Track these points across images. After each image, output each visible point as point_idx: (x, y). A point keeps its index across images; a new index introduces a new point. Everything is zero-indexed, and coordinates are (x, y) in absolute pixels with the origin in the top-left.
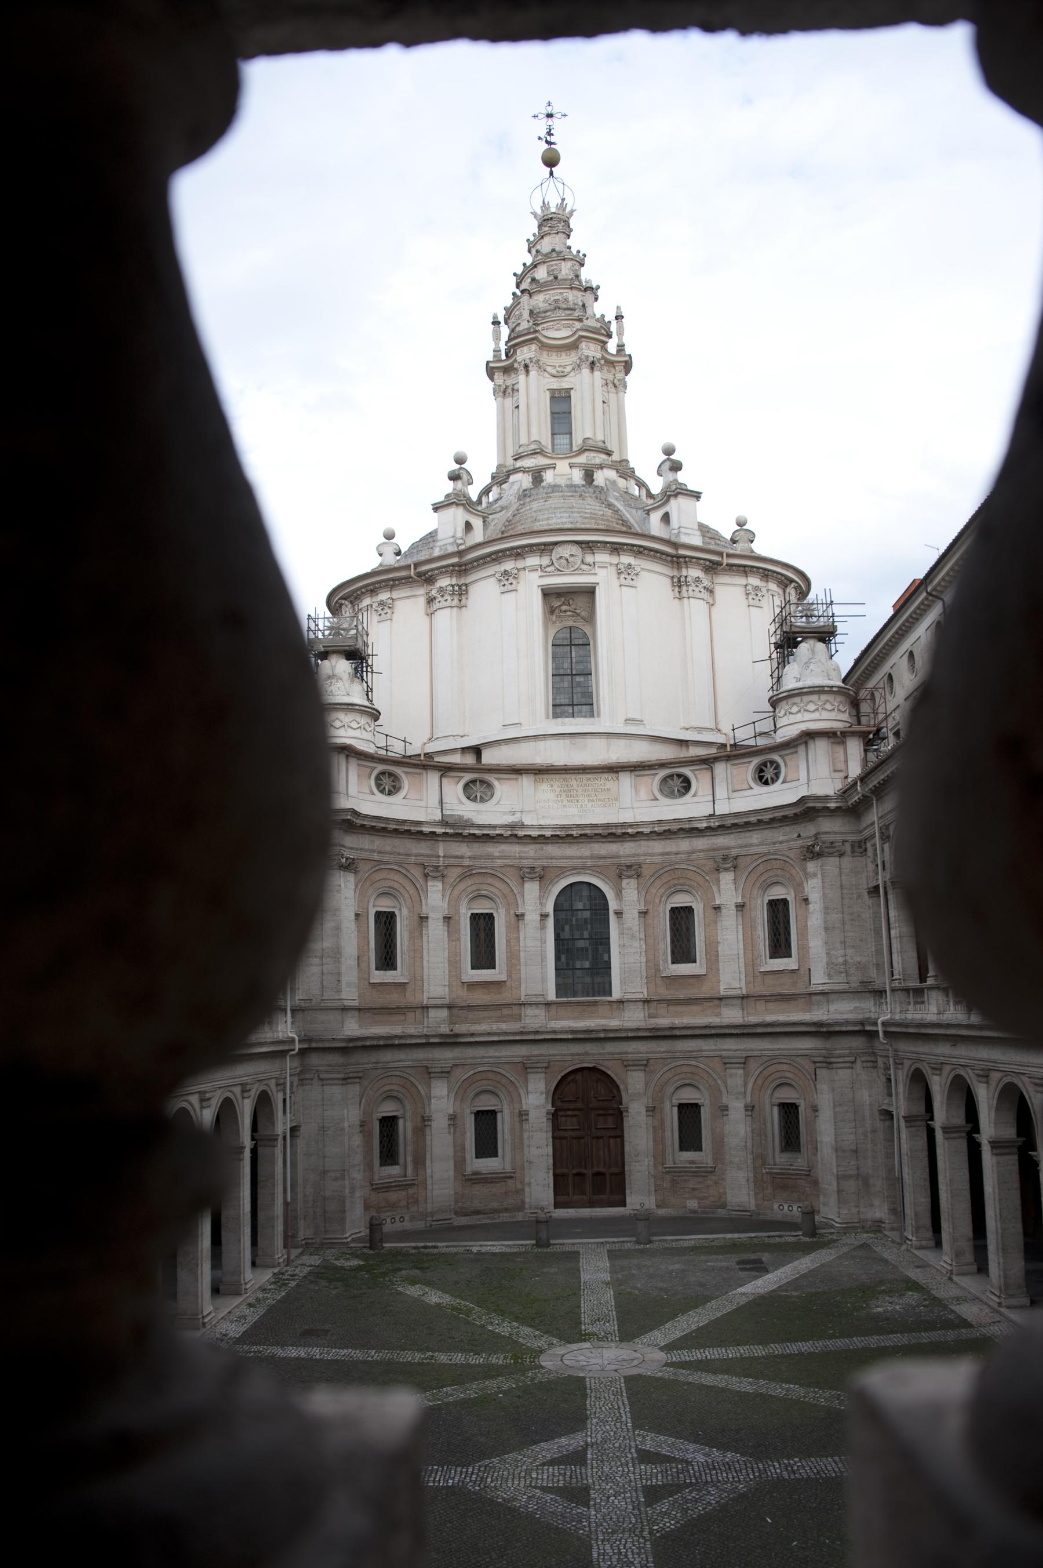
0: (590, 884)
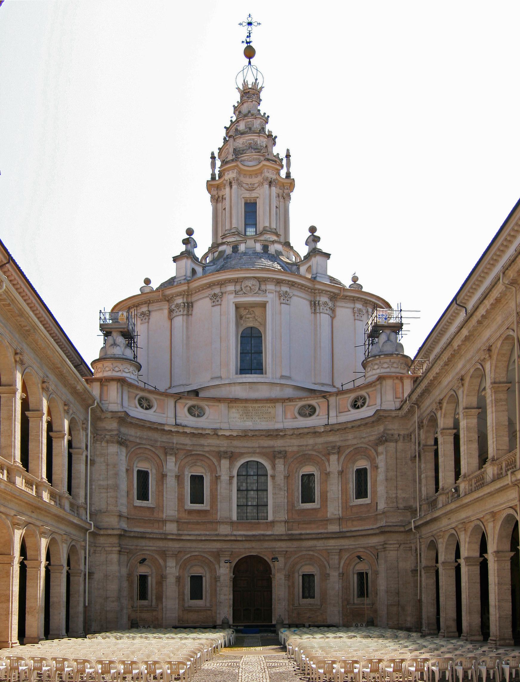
0: (258, 462)
